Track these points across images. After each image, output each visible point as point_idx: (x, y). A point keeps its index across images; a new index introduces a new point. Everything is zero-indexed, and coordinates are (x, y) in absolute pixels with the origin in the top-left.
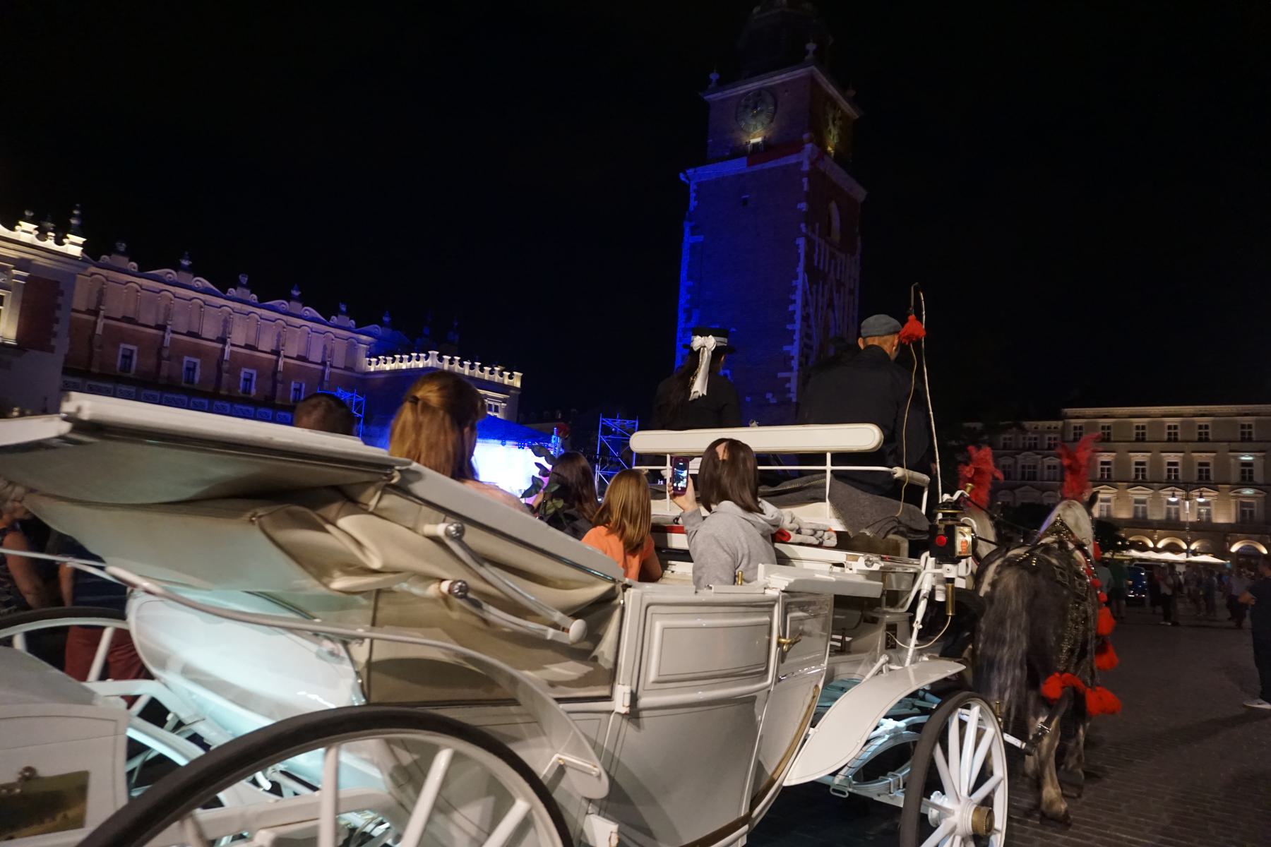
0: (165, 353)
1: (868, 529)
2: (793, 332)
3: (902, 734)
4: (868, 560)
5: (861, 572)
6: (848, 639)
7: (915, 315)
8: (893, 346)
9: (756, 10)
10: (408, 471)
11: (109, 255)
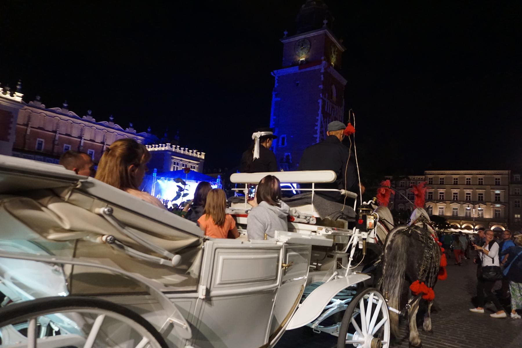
0: (56, 142)
1: (329, 216)
2: (316, 138)
3: (343, 306)
4: (326, 230)
5: (323, 235)
6: (319, 265)
7: (351, 123)
8: (341, 135)
9: (303, 6)
10: (87, 182)
11: (33, 101)
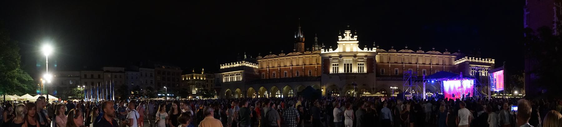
11: (390, 50)
